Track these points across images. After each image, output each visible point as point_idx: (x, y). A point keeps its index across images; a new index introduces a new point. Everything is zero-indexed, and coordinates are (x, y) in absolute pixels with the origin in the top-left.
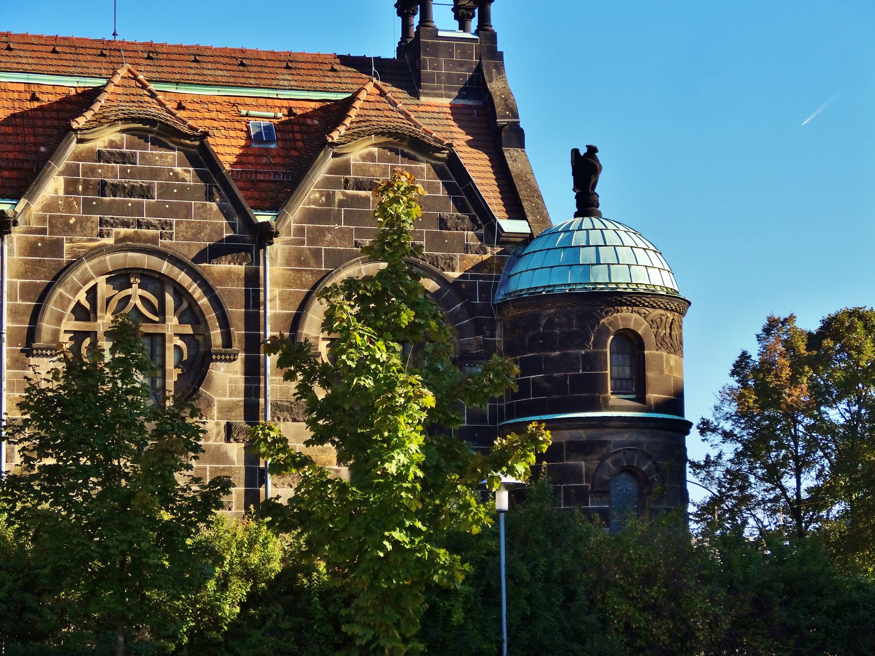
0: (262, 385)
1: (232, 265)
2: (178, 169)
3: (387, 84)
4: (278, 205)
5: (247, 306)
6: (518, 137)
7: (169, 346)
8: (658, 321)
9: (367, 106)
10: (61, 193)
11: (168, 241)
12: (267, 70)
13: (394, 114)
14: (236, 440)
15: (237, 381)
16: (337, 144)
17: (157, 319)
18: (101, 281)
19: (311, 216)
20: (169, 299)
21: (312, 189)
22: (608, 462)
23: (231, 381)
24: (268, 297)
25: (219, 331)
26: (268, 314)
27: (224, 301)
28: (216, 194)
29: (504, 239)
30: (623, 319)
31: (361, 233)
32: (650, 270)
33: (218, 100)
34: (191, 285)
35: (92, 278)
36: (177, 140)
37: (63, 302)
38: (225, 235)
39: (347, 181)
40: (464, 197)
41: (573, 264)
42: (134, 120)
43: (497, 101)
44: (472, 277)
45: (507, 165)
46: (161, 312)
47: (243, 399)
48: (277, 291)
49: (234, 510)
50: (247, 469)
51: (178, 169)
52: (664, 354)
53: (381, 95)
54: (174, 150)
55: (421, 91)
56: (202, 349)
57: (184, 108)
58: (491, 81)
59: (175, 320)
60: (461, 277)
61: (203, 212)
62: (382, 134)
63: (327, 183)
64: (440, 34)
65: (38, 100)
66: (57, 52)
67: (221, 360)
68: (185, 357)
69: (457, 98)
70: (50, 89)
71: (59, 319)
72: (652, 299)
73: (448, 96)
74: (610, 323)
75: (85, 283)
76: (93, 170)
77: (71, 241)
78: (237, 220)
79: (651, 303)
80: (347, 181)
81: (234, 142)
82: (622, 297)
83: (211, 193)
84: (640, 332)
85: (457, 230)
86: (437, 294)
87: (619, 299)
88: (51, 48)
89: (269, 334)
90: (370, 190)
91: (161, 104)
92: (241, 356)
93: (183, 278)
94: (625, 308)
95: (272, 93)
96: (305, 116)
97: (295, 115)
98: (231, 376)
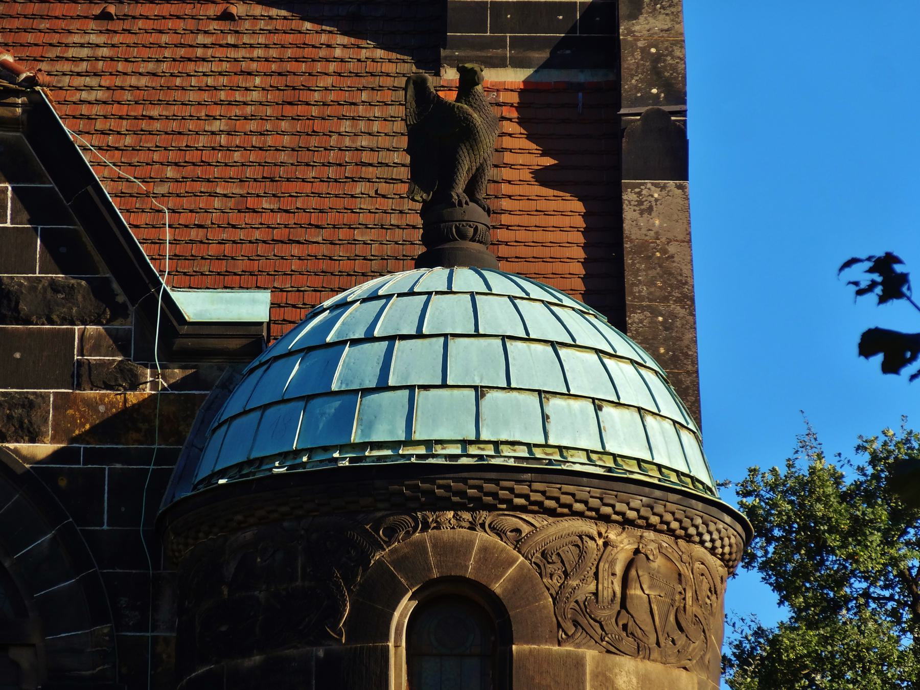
3: (363, 43)
8: (570, 554)
12: (44, 25)
29: (189, 343)
32: (555, 405)
40: (80, 228)
43: (630, 60)
44: (91, 455)
45: (620, 220)
52: (591, 655)
55: (443, 53)
58: (634, 15)
60: (55, 456)
69: (547, 65)
72: (536, 486)
73: (518, 63)
74: (401, 561)
79: (535, 497)
82: (433, 482)
84: (497, 587)
85: (51, 322)
87: (427, 486)
94: (450, 514)
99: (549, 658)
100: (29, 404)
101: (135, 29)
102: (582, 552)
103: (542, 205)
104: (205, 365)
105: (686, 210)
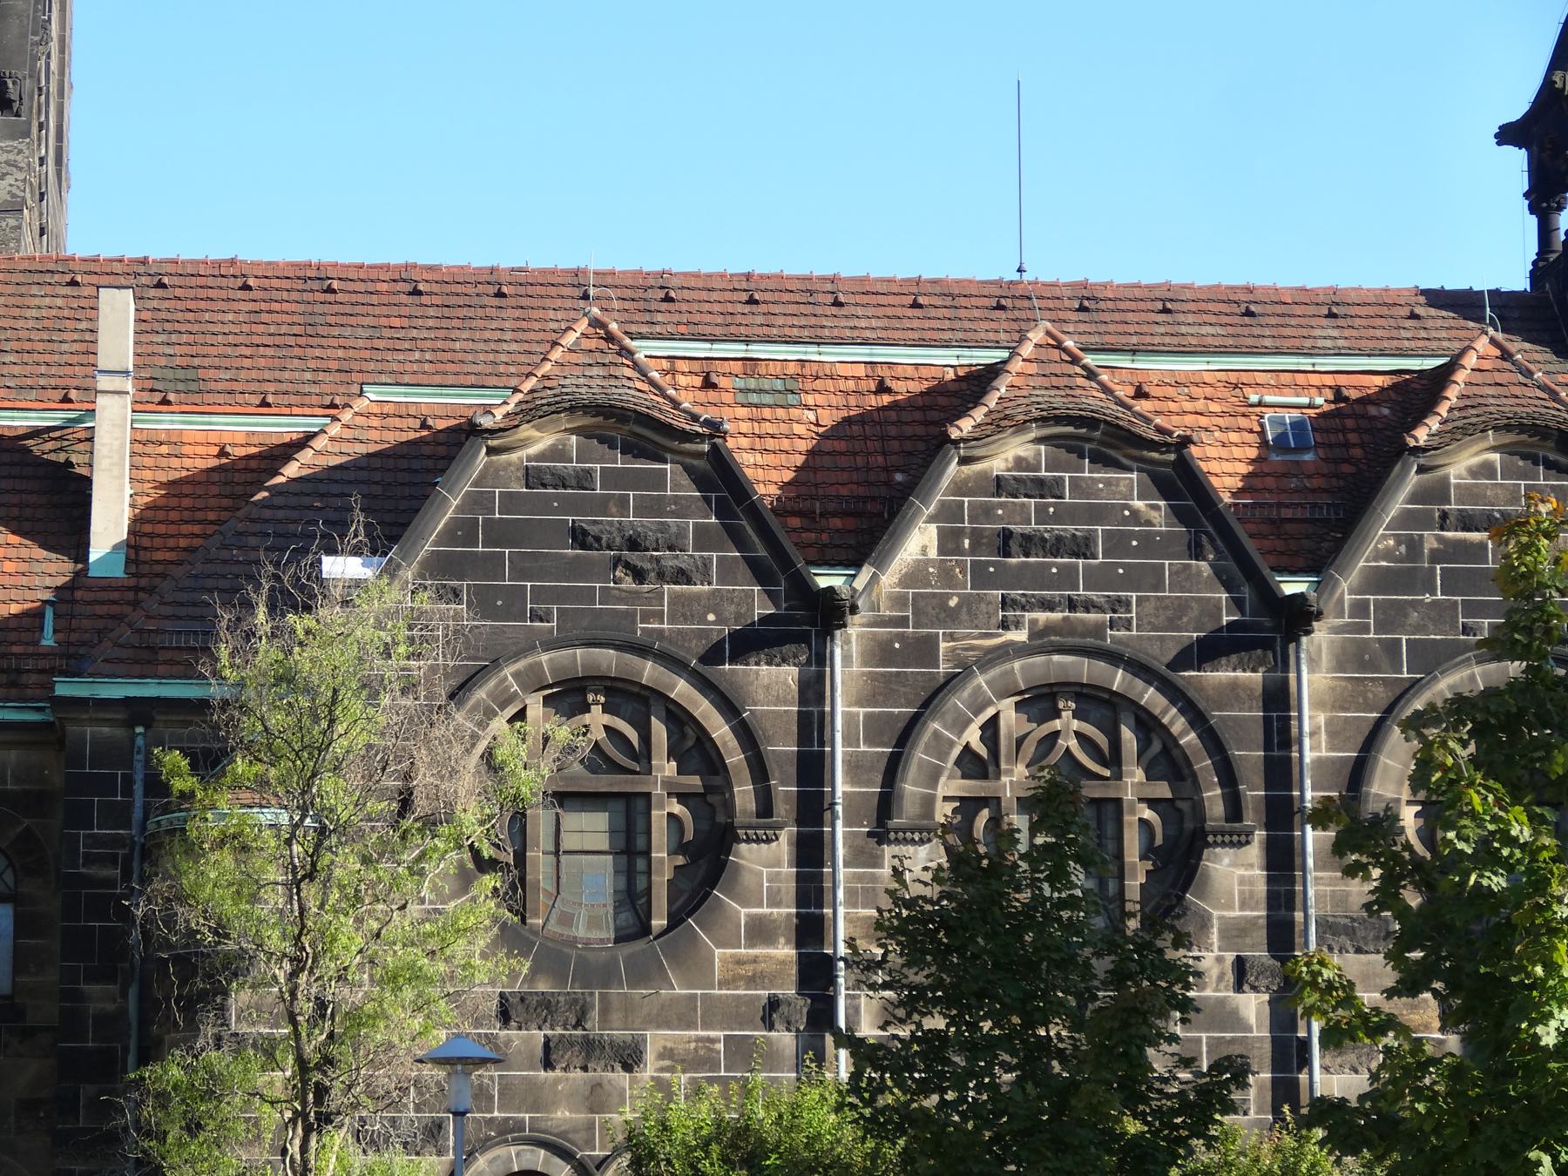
0: (1298, 888)
1: (1239, 674)
2: (1139, 504)
4: (1318, 564)
5: (1268, 746)
7: (658, 817)
9: (1478, 378)
10: (933, 553)
11: (1122, 633)
12: (1293, 322)
13: (1529, 392)
14: (1255, 989)
16: (1424, 450)
17: (1107, 773)
19: (1378, 581)
20: (1127, 735)
21: (1381, 532)
23: (1242, 881)
24: (1306, 728)
25: (1219, 791)
26: (1307, 760)
27: (1226, 736)
28: (1208, 547)
31: (1472, 609)
33: (1208, 378)
34: (1165, 712)
35: (990, 703)
36: (1135, 452)
37: (940, 746)
38: (1225, 619)
39: (1444, 515)
42: (1058, 420)
46: (1114, 759)
47: (1264, 913)
48: (1322, 718)
49: (1252, 1114)
50: (1274, 1040)
51: (1139, 504)
53: (1503, 358)
54: (1130, 470)
56: (1189, 825)
57: (1146, 396)
59: (1139, 775)
61: (1183, 578)
62: (1508, 428)
63: (1406, 519)
65: (889, 391)
66: (756, 302)
67: (1223, 844)
68: (1159, 841)
70: (910, 372)
71: (933, 777)
75: (978, 711)
76: (986, 512)
77: (952, 637)
78: (1246, 592)
80: (1444, 515)
81: (1237, 453)
83: (1199, 545)
88: (744, 297)
89: (1309, 795)
90: (1486, 530)
91: (1105, 389)
92: (1260, 835)
93: (1150, 697)
95: (1305, 363)
96: (1364, 401)
97: (1346, 399)
98: (1242, 872)
101: (1356, 325)
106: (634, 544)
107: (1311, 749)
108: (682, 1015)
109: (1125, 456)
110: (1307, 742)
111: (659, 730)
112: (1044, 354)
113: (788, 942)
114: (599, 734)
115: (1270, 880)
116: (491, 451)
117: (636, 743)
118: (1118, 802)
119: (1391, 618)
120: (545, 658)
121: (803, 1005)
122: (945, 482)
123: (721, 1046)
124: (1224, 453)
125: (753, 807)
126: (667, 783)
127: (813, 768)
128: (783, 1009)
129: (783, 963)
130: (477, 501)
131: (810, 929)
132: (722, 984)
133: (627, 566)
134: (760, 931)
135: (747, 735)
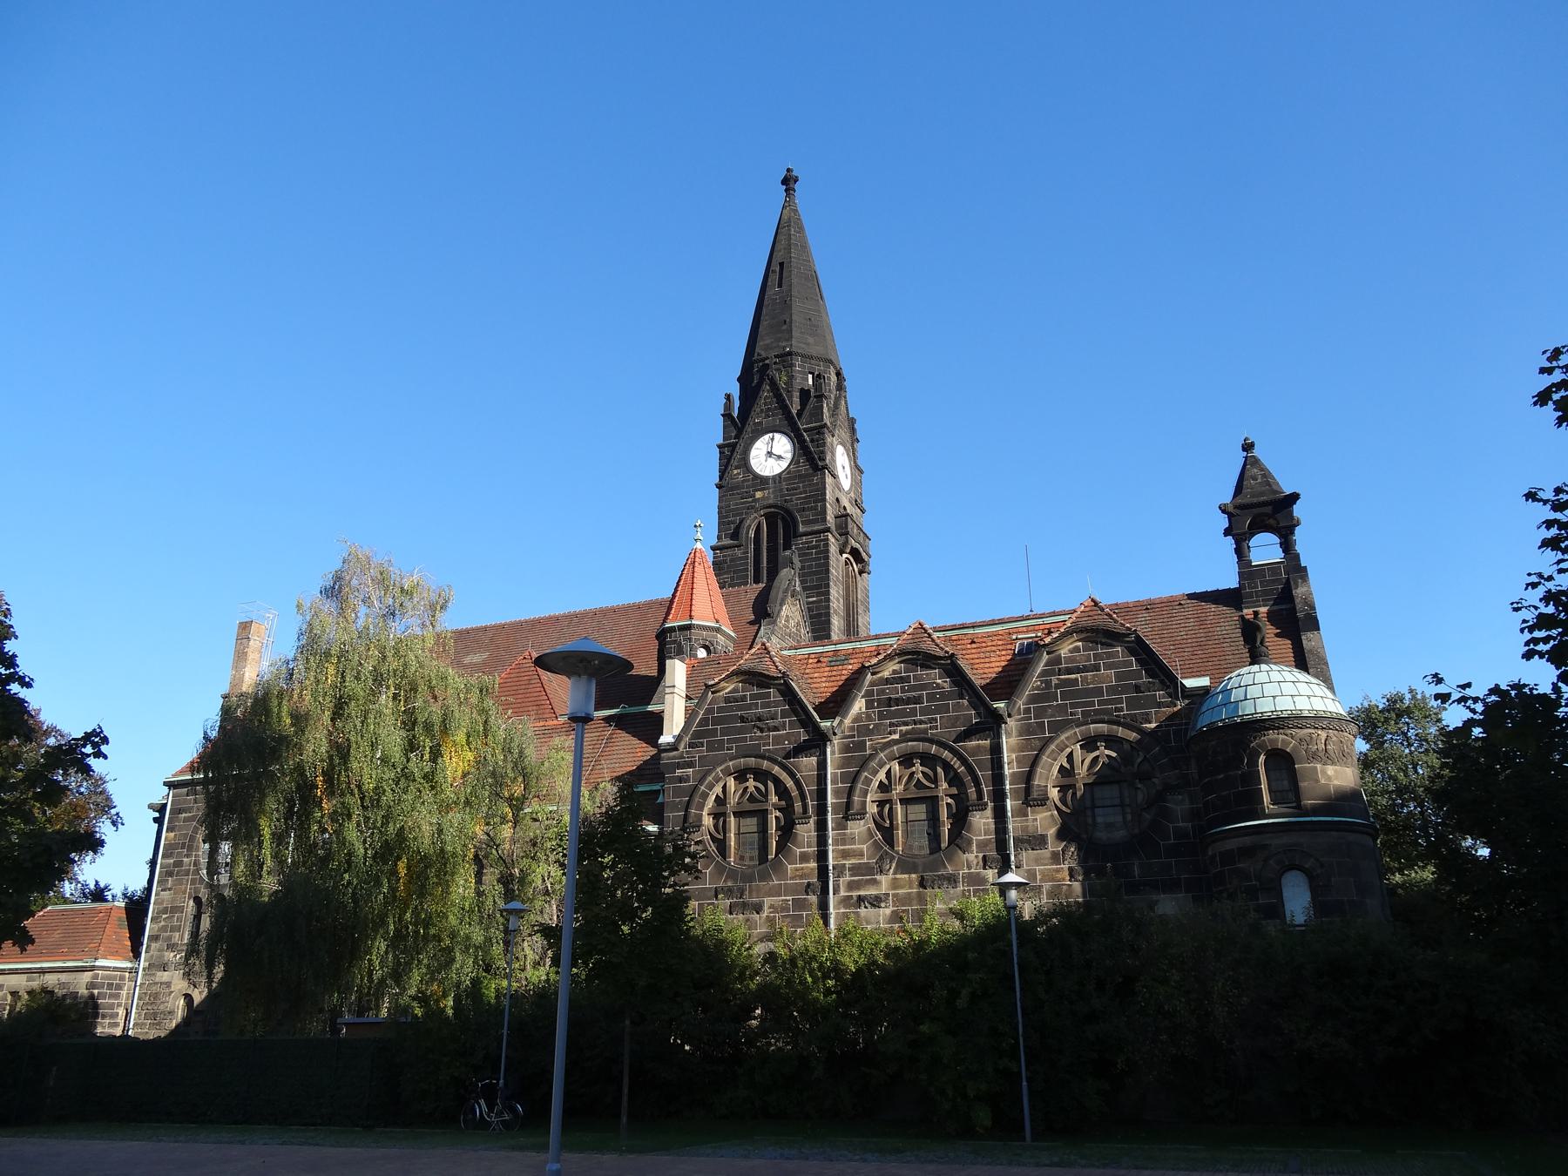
1: (980, 742)
6: (1313, 624)
8: (1308, 739)
10: (864, 710)
14: (991, 868)
15: (988, 824)
16: (1048, 645)
17: (933, 786)
18: (896, 767)
19: (1033, 699)
20: (939, 770)
22: (1271, 862)
25: (974, 789)
28: (965, 694)
30: (1270, 740)
31: (1073, 706)
32: (1296, 699)
34: (952, 760)
37: (868, 782)
39: (1060, 670)
41: (1227, 703)
43: (1297, 601)
46: (935, 781)
52: (1319, 766)
53: (1095, 606)
59: (945, 785)
60: (1155, 728)
61: (957, 707)
62: (1081, 631)
64: (1253, 564)
67: (976, 810)
68: (954, 811)
69: (1273, 605)
71: (865, 793)
74: (1259, 745)
76: (882, 692)
77: (871, 740)
78: (982, 710)
80: (1060, 670)
81: (1003, 658)
83: (962, 694)
84: (1288, 750)
86: (1139, 742)
89: (1008, 787)
91: (933, 640)
92: (990, 805)
93: (946, 754)
99: (1305, 768)
100: (1147, 714)
102: (1311, 738)
103: (1281, 643)
104: (1194, 698)
105: (1321, 638)
106: (759, 719)
107: (1009, 769)
108: (777, 892)
109: (934, 664)
110: (1006, 766)
111: (771, 786)
112: (916, 631)
113: (814, 861)
114: (752, 789)
115: (996, 823)
116: (713, 693)
117: (763, 790)
118: (938, 796)
119: (1040, 713)
120: (731, 763)
121: (819, 885)
122: (867, 683)
123: (790, 903)
124: (998, 659)
125: (801, 811)
126: (773, 805)
127: (821, 794)
128: (811, 887)
129: (812, 869)
130: (709, 711)
131: (822, 856)
132: (792, 879)
133: (758, 727)
134: (804, 858)
135: (798, 783)
